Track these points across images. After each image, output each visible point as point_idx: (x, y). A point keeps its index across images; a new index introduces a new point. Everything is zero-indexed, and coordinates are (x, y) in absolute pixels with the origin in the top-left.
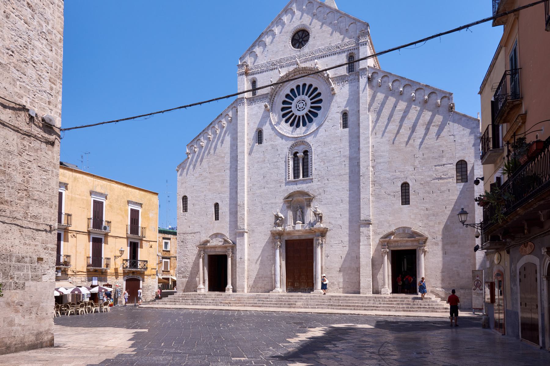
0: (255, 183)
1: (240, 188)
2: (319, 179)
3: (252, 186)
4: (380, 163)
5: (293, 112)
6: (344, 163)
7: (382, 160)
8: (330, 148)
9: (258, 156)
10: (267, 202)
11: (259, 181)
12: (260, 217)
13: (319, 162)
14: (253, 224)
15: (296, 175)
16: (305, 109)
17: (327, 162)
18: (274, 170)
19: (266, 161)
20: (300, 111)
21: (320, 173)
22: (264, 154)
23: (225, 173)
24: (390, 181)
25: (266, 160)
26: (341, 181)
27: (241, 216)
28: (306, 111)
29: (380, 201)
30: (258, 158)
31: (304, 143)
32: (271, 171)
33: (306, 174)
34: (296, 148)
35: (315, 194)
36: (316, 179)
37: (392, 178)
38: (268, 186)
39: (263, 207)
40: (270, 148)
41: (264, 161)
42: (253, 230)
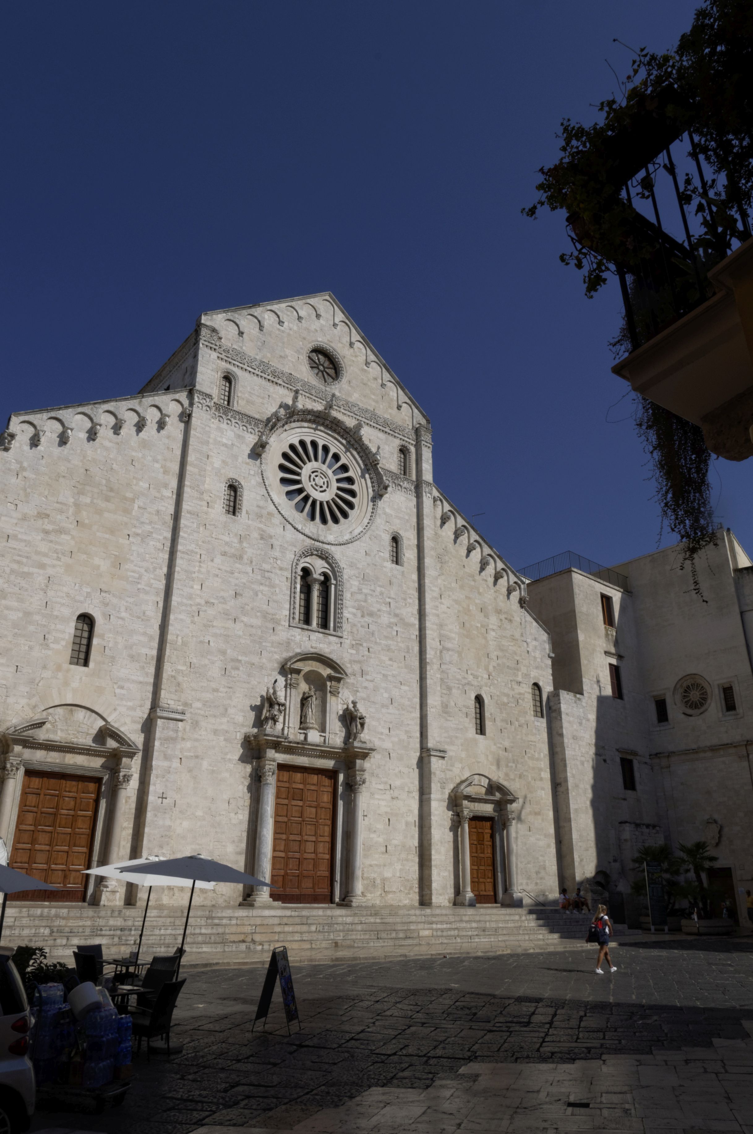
0: (212, 601)
1: (179, 600)
2: (354, 642)
3: (203, 602)
4: (448, 650)
5: (335, 491)
6: (395, 628)
7: (449, 645)
8: (372, 588)
9: (226, 538)
10: (240, 658)
11: (223, 598)
12: (216, 690)
13: (353, 607)
14: (198, 705)
16: (327, 492)
17: (368, 614)
18: (262, 588)
19: (245, 560)
21: (354, 630)
22: (241, 542)
23: (127, 542)
24: (461, 687)
25: (245, 557)
26: (391, 659)
27: (173, 674)
29: (449, 718)
30: (227, 543)
31: (324, 556)
32: (256, 587)
33: (324, 624)
34: (308, 559)
37: (464, 681)
38: (245, 619)
39: (229, 667)
40: (255, 535)
41: (241, 558)
42: (197, 722)
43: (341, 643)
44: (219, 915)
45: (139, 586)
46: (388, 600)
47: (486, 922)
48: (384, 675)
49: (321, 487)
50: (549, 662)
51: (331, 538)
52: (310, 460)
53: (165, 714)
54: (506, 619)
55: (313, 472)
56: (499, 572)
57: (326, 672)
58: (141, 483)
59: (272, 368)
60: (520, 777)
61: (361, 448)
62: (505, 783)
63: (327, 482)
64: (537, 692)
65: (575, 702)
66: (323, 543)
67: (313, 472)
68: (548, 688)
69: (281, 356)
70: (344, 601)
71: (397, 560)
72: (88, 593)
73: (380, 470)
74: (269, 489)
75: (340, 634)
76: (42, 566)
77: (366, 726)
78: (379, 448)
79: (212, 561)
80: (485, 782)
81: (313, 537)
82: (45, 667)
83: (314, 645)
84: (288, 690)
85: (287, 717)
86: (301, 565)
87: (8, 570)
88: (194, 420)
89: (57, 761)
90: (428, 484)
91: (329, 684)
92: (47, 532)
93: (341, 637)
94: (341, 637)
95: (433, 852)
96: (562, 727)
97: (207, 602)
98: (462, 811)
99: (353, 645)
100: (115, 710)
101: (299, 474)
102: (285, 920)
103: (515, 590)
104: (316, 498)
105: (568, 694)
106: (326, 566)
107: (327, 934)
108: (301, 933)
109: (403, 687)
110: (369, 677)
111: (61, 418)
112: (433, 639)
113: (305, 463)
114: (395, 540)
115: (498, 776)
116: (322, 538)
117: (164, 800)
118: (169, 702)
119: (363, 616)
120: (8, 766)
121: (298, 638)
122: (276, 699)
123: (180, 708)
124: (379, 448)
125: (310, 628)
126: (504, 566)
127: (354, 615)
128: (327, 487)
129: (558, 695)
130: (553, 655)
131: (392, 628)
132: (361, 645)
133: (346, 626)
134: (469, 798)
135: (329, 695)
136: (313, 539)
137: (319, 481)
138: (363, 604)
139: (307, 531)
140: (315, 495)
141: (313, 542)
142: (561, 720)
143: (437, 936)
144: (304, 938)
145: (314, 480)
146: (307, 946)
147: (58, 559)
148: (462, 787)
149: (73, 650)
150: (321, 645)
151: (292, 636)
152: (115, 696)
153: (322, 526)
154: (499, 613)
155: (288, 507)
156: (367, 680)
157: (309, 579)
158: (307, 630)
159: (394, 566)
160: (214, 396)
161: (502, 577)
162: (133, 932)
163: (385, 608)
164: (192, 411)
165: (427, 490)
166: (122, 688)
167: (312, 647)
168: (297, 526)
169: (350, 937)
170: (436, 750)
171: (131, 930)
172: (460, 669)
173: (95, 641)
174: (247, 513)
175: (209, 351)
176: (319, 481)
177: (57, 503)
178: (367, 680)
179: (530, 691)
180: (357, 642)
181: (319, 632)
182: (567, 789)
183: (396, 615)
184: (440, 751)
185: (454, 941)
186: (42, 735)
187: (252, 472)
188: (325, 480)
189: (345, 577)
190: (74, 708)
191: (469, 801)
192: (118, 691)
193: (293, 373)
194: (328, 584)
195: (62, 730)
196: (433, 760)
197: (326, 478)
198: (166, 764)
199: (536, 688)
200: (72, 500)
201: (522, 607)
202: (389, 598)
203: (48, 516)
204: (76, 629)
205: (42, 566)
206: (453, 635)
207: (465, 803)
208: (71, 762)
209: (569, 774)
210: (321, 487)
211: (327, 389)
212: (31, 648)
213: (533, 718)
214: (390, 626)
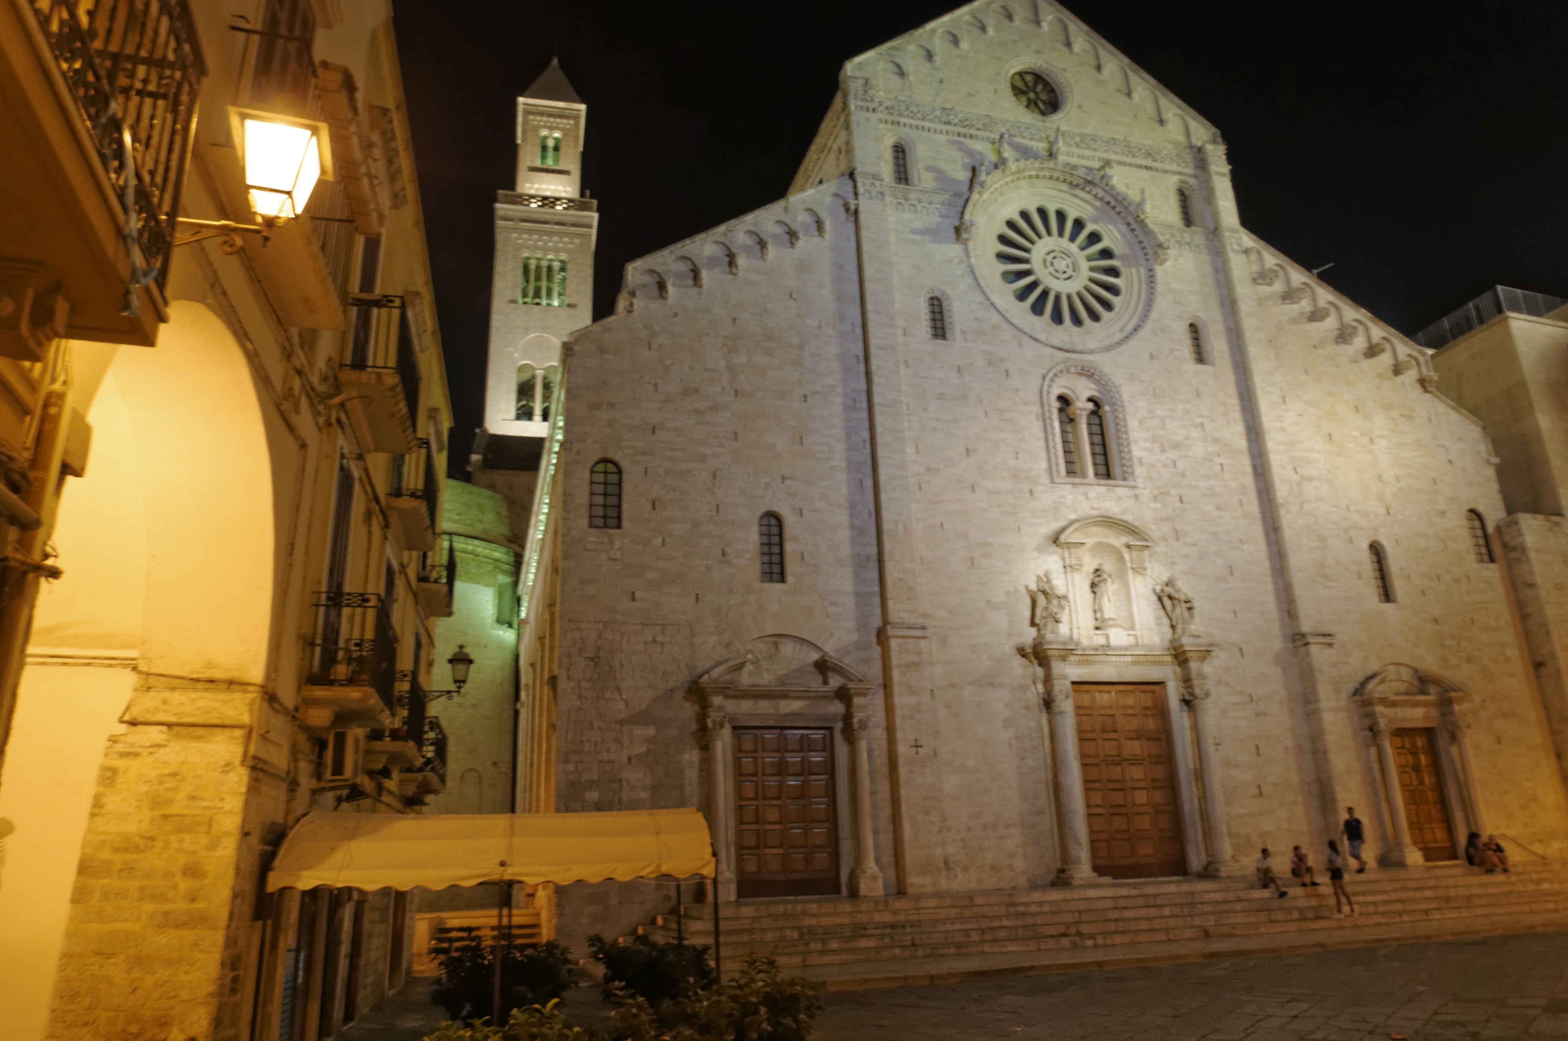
2: (1156, 492)
4: (1310, 479)
6: (1218, 461)
7: (1310, 472)
26: (1218, 508)
31: (1087, 373)
36: (1144, 492)
43: (1136, 496)
44: (1024, 900)
45: (833, 463)
46: (1199, 420)
47: (1448, 887)
48: (1212, 533)
49: (1064, 272)
50: (1491, 472)
51: (1091, 345)
52: (1039, 236)
53: (900, 632)
54: (1402, 416)
55: (1048, 254)
56: (1378, 344)
57: (1119, 541)
58: (808, 321)
59: (961, 115)
60: (1469, 660)
61: (1116, 200)
62: (1446, 674)
63: (1073, 263)
64: (1477, 524)
65: (1550, 530)
66: (1082, 352)
67: (1048, 254)
68: (1494, 513)
69: (970, 95)
70: (1131, 433)
71: (1200, 357)
72: (766, 484)
73: (1151, 226)
74: (987, 291)
75: (1131, 483)
76: (702, 458)
77: (1196, 612)
78: (1142, 192)
79: (925, 410)
80: (1406, 675)
81: (1066, 347)
82: (731, 591)
83: (1095, 505)
84: (1069, 574)
85: (1073, 615)
86: (1056, 391)
87: (661, 471)
88: (863, 217)
89: (771, 711)
90: (1235, 231)
91: (1127, 556)
92: (698, 412)
93: (1134, 487)
94: (1134, 487)
95: (1338, 789)
96: (1531, 573)
97: (929, 470)
98: (1376, 723)
99: (1155, 496)
100: (832, 635)
101: (1026, 261)
102: (1122, 903)
103: (1408, 368)
104: (1060, 290)
105: (1534, 518)
106: (1093, 386)
107: (1188, 918)
108: (1150, 919)
109: (1245, 547)
110: (1189, 540)
111: (688, 255)
112: (1283, 467)
113: (1032, 242)
114: (1194, 328)
115: (1430, 663)
116: (1079, 347)
117: (919, 749)
118: (902, 615)
119: (1163, 451)
120: (710, 724)
121: (1069, 499)
122: (1052, 589)
123: (919, 621)
124: (1142, 192)
125: (1084, 481)
126: (1384, 334)
127: (1150, 451)
128: (1074, 271)
129: (1516, 523)
130: (1495, 460)
131: (1211, 460)
132: (1168, 494)
133: (1138, 470)
134: (1384, 701)
135: (1130, 573)
136: (1067, 351)
137: (1061, 264)
138: (1160, 432)
139: (1055, 342)
140: (1058, 286)
141: (1067, 355)
142: (1528, 561)
143: (1369, 914)
144: (1156, 926)
145: (1052, 264)
146: (1162, 937)
147: (721, 445)
148: (1371, 685)
149: (763, 563)
150: (1107, 504)
151: (1061, 497)
152: (829, 617)
153: (1076, 330)
154: (1388, 409)
155: (1021, 312)
156: (1186, 544)
157: (1070, 410)
158: (1082, 484)
159: (1199, 367)
160: (884, 176)
161: (1383, 351)
162: (908, 930)
163: (1196, 433)
164: (857, 205)
165: (1233, 241)
166: (834, 604)
167: (1093, 509)
168: (1039, 337)
169: (1226, 922)
170: (1317, 635)
171: (904, 926)
172: (1335, 506)
173: (789, 547)
174: (963, 332)
175: (865, 114)
176: (1061, 264)
177: (706, 370)
178: (1186, 544)
179: (1464, 522)
180: (1162, 490)
181: (1099, 485)
182: (1558, 671)
183: (1216, 441)
184: (1324, 635)
185: (1398, 919)
186: (745, 679)
187: (959, 273)
188: (1069, 261)
189: (1125, 397)
190: (778, 640)
191: (1385, 706)
192: (831, 609)
193: (991, 114)
194: (1101, 413)
195: (768, 671)
196: (1314, 650)
197: (1069, 257)
198: (913, 700)
199: (1474, 517)
200: (722, 363)
201: (1426, 391)
202: (1200, 416)
203: (696, 391)
204: (762, 535)
205: (702, 458)
206: (1315, 456)
207: (1379, 709)
208: (788, 711)
209: (1558, 647)
210: (1064, 272)
211: (1048, 125)
212: (708, 568)
213: (1476, 566)
214: (1209, 458)
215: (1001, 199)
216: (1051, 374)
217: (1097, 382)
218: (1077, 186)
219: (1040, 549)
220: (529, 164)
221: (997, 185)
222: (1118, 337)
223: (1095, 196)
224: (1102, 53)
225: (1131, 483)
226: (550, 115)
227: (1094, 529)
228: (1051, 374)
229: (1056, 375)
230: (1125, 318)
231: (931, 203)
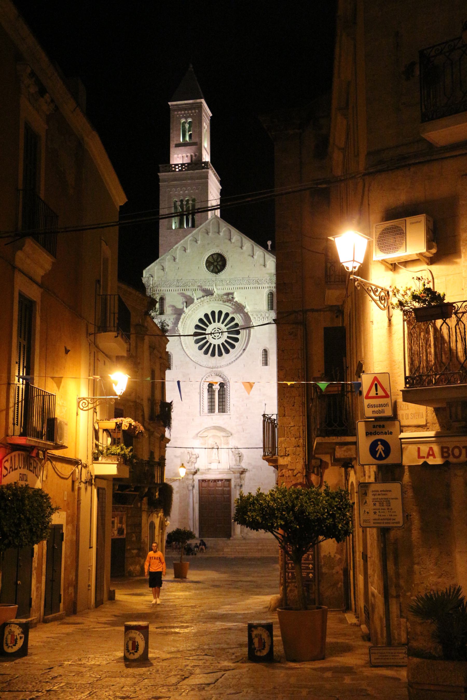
15: (211, 410)
20: (215, 339)
28: (222, 340)
33: (222, 410)
35: (233, 432)
174: (176, 366)
215: (196, 312)
216: (205, 377)
217: (222, 378)
218: (225, 302)
219: (194, 438)
220: (175, 142)
221: (194, 308)
222: (234, 359)
223: (232, 304)
224: (244, 239)
225: (229, 413)
226: (185, 109)
227: (212, 431)
228: (205, 377)
229: (207, 377)
230: (238, 351)
231: (169, 319)
